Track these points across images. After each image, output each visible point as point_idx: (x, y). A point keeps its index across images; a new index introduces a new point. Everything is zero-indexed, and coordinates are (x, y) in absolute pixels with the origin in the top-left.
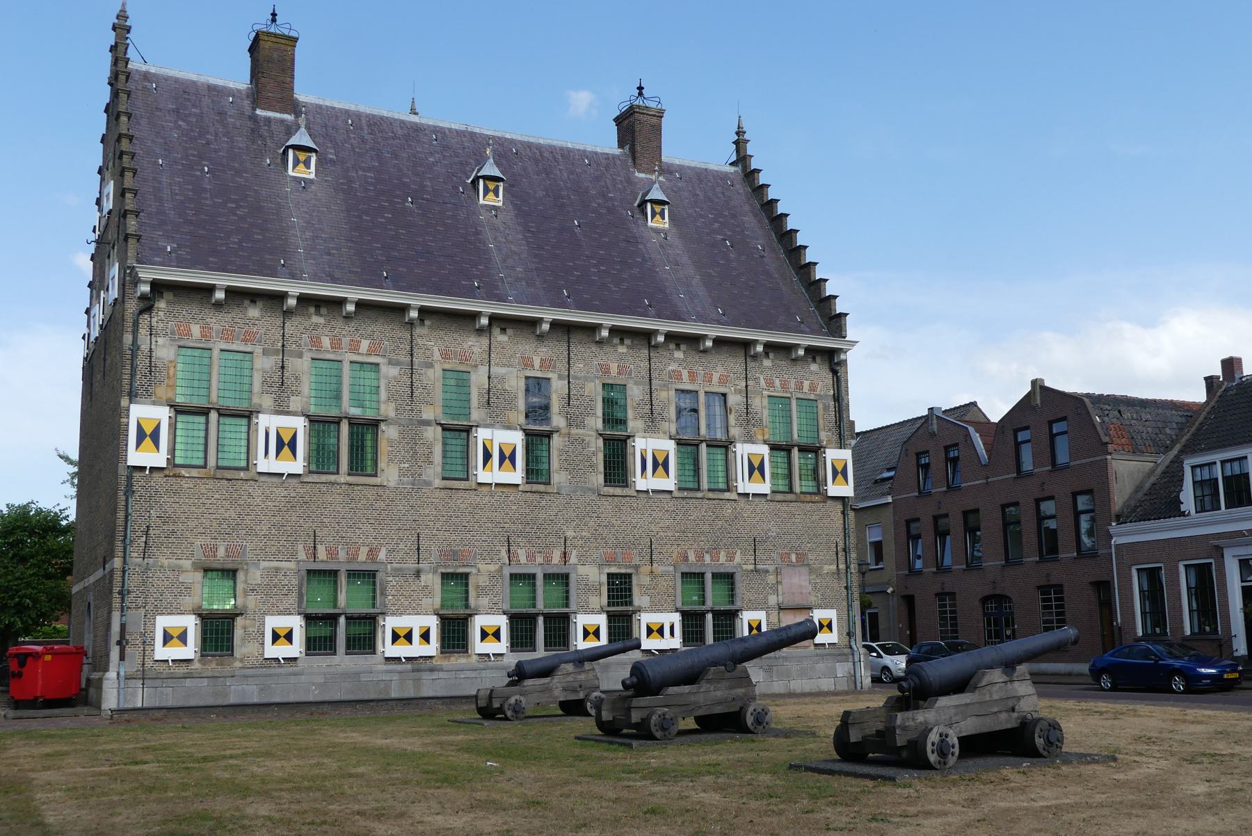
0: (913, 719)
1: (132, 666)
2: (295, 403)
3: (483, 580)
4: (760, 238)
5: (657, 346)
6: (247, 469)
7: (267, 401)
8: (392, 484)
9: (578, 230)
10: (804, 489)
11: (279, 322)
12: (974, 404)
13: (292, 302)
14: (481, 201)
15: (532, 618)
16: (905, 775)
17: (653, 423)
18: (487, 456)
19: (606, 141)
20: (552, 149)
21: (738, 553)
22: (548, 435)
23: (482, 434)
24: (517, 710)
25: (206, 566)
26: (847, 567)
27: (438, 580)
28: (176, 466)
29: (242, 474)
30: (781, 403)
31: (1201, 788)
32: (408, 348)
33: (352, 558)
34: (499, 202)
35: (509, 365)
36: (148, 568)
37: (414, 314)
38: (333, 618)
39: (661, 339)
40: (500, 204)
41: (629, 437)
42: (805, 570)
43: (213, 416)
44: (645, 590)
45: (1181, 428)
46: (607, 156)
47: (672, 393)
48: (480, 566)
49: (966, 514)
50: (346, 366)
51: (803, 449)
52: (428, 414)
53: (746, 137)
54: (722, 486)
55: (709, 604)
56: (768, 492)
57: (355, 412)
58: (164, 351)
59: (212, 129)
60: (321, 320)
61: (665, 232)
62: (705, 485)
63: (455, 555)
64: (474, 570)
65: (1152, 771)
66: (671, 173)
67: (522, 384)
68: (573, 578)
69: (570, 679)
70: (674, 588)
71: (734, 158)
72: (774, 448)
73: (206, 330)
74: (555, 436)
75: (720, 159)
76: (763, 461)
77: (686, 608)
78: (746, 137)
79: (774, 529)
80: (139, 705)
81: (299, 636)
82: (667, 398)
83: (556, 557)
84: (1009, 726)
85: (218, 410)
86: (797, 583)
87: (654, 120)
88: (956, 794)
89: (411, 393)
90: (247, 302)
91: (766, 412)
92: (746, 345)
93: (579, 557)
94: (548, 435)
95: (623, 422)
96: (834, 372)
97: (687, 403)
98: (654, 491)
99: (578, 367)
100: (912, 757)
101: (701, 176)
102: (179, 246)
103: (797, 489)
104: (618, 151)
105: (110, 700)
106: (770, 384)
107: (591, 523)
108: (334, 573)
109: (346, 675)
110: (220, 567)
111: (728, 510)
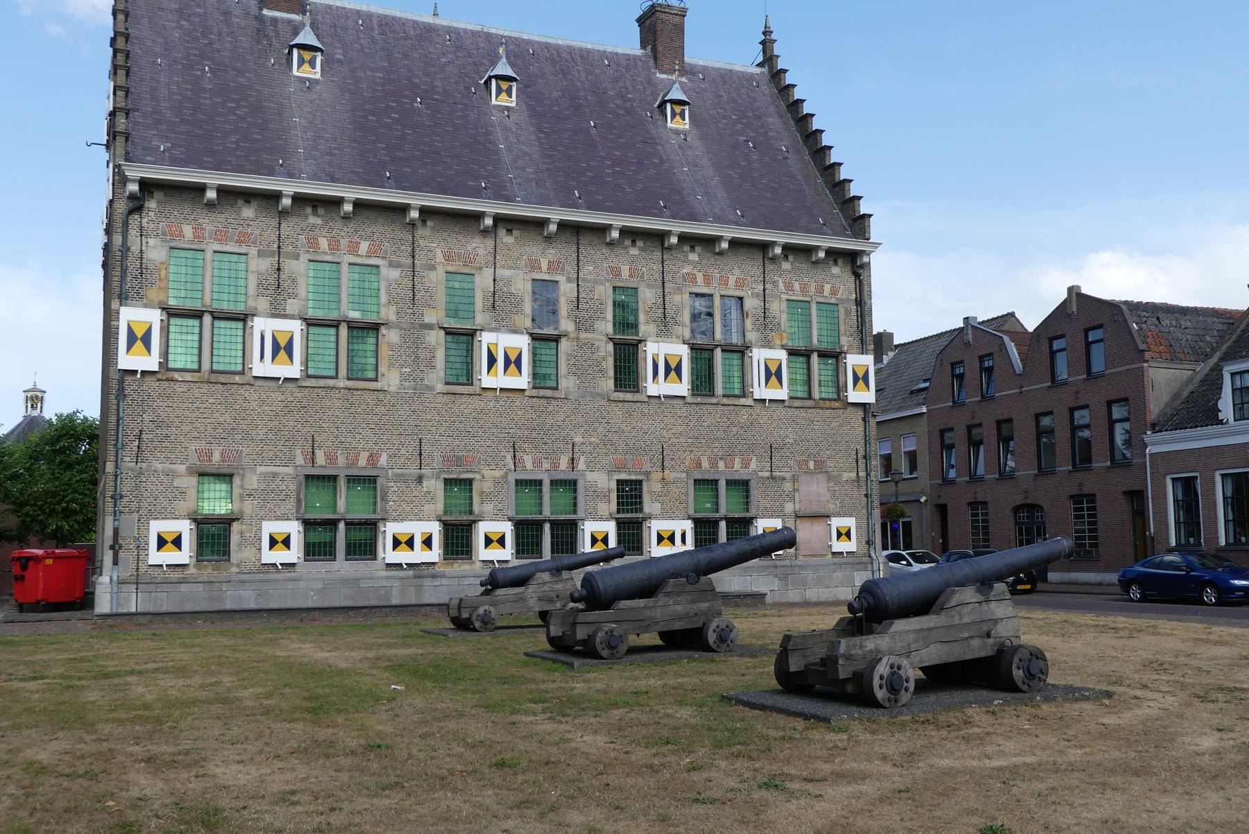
0: (861, 647)
1: (126, 570)
2: (292, 306)
3: (487, 486)
4: (785, 140)
5: (670, 248)
6: (242, 373)
7: (263, 304)
8: (393, 389)
9: (593, 131)
10: (824, 396)
11: (274, 223)
12: (1012, 315)
13: (287, 202)
14: (494, 102)
15: (539, 525)
16: (841, 714)
17: (665, 327)
18: (492, 360)
19: (628, 42)
20: (571, 50)
21: (754, 459)
22: (556, 339)
23: (486, 338)
24: (486, 621)
25: (201, 470)
26: (868, 475)
27: (441, 485)
28: (168, 370)
29: (237, 379)
30: (799, 307)
31: (1208, 742)
32: (410, 249)
33: (352, 464)
34: (512, 102)
35: (517, 268)
36: (141, 473)
37: (414, 214)
38: (333, 524)
39: (674, 240)
40: (514, 105)
41: (640, 341)
42: (823, 478)
43: (207, 319)
44: (656, 497)
45: (1222, 336)
46: (628, 57)
47: (686, 296)
48: (485, 472)
49: (999, 423)
50: (345, 268)
51: (823, 355)
52: (430, 317)
53: (773, 36)
54: (737, 392)
55: (723, 511)
56: (786, 398)
57: (355, 315)
58: (155, 252)
59: (215, 29)
60: (319, 221)
61: (685, 133)
62: (719, 390)
63: (458, 461)
64: (478, 477)
65: (1153, 712)
66: (694, 74)
67: (529, 286)
68: (580, 485)
69: (546, 588)
70: (687, 495)
71: (760, 59)
72: (792, 353)
73: (198, 230)
74: (563, 341)
75: (746, 60)
76: (780, 366)
77: (698, 515)
78: (773, 36)
80: (133, 610)
81: (297, 542)
82: (682, 304)
83: (564, 463)
84: (983, 654)
85: (211, 313)
86: (815, 491)
87: (677, 19)
88: (893, 744)
89: (413, 296)
90: (241, 202)
91: (784, 317)
92: (764, 247)
93: (588, 463)
94: (556, 339)
95: (634, 326)
96: (857, 276)
97: (700, 305)
98: (665, 397)
99: (588, 270)
100: (855, 693)
101: (726, 77)
102: (174, 146)
103: (816, 395)
104: (639, 52)
105: (103, 604)
106: (789, 287)
107: (601, 429)
108: (333, 479)
109: (345, 581)
110: (215, 471)
111: (744, 416)
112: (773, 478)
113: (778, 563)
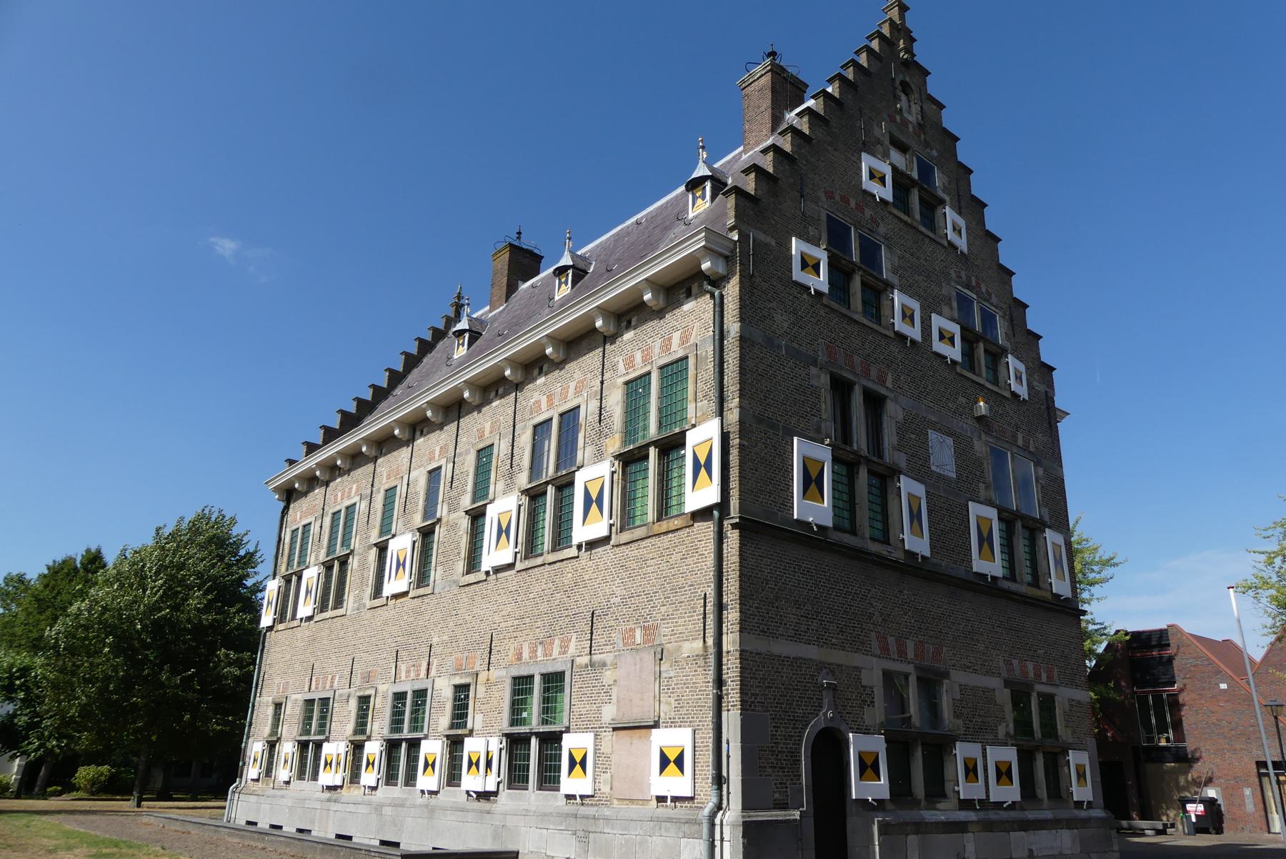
106: (630, 364)
112: (592, 664)
113: (583, 810)
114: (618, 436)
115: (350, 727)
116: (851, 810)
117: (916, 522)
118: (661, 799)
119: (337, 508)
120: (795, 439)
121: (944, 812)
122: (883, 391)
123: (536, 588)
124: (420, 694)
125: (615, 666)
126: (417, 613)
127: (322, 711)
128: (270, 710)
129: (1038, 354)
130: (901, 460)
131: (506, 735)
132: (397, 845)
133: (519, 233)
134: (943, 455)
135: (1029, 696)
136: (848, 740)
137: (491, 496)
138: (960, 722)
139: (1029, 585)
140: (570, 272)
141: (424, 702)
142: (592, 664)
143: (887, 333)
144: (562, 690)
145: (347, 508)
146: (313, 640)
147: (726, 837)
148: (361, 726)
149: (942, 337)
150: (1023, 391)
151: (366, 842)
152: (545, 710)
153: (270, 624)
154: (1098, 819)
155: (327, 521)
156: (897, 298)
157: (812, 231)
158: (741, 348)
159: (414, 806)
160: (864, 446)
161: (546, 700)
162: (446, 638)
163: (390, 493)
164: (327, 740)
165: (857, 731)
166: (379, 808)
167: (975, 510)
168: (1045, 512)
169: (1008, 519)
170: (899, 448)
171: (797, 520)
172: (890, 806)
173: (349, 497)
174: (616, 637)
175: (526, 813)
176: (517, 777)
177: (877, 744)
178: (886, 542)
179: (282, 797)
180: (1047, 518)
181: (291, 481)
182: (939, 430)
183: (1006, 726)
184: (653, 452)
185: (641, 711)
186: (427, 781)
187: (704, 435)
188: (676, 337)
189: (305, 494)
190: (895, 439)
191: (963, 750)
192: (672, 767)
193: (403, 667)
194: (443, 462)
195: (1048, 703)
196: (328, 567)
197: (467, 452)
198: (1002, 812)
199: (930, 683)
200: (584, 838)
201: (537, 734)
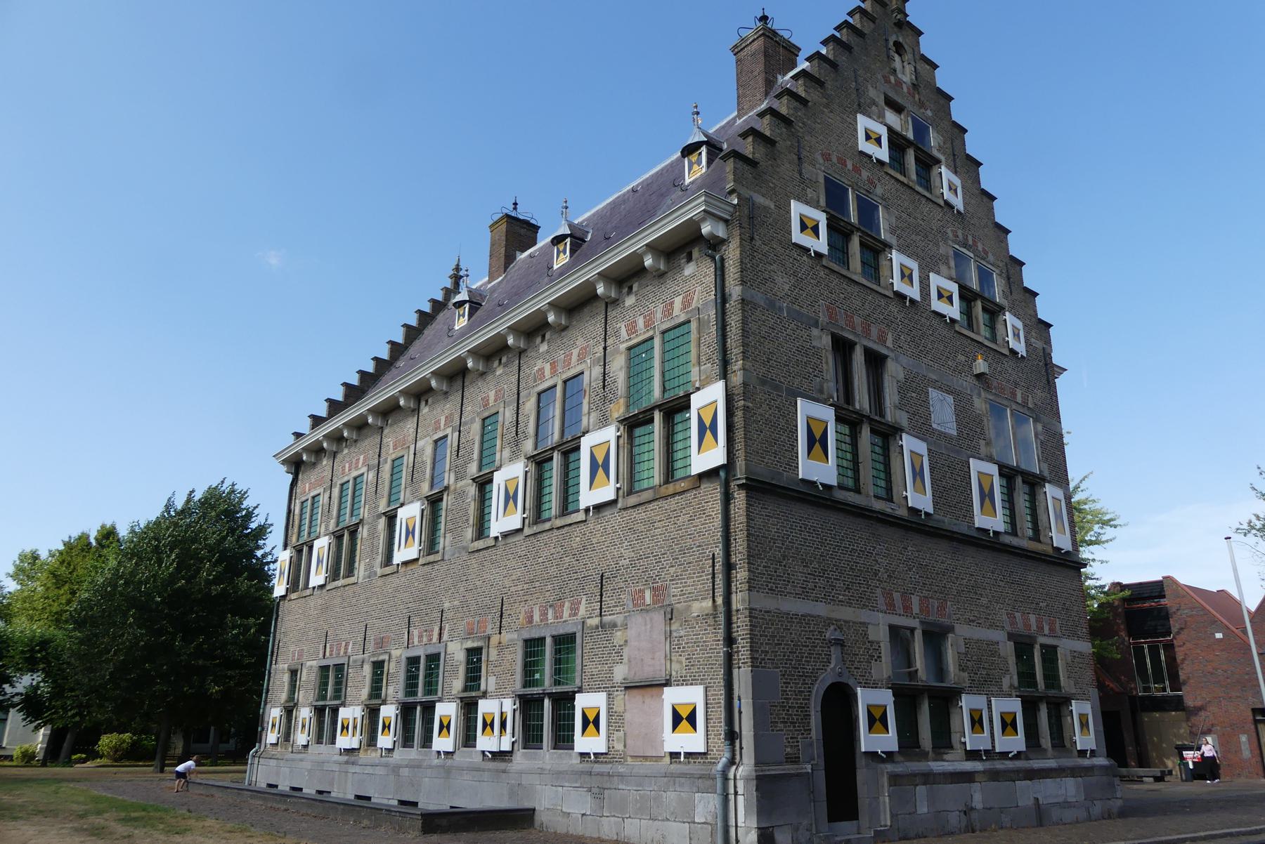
79: (627, 554)
106: (632, 329)
112: (602, 625)
113: (598, 768)
114: (622, 401)
115: (365, 692)
116: (861, 762)
117: (918, 478)
118: (674, 755)
119: (346, 479)
120: (799, 401)
121: (953, 763)
122: (884, 351)
123: (545, 553)
124: (433, 659)
125: (625, 627)
126: (428, 579)
127: (337, 677)
128: (286, 678)
129: (1035, 311)
130: (903, 419)
131: (520, 697)
132: (415, 804)
133: (515, 204)
134: (943, 413)
135: (1031, 646)
136: (856, 694)
137: (497, 463)
138: (966, 674)
139: (1030, 539)
140: (568, 240)
141: (438, 666)
142: (602, 625)
143: (887, 293)
144: (573, 650)
145: (355, 479)
146: (325, 608)
147: (740, 791)
148: (376, 691)
149: (940, 296)
150: (1021, 348)
151: (385, 802)
152: (557, 672)
153: (283, 593)
154: (1102, 767)
155: (336, 491)
156: (897, 258)
157: (810, 193)
158: (743, 310)
159: (430, 767)
160: (866, 406)
161: (557, 661)
162: (456, 603)
163: (396, 463)
164: (343, 705)
165: (866, 685)
166: (396, 769)
167: (976, 466)
168: (1045, 467)
169: (1008, 474)
170: (899, 407)
171: (802, 480)
172: (898, 758)
173: (357, 468)
174: (625, 597)
175: (541, 772)
176: (531, 737)
177: (885, 698)
178: (890, 500)
179: (301, 760)
180: (1046, 474)
181: (298, 454)
182: (940, 388)
183: (1010, 679)
184: (657, 416)
185: (654, 668)
186: (443, 743)
187: (709, 397)
188: (678, 301)
189: (314, 465)
190: (896, 398)
191: (967, 702)
192: (685, 723)
193: (415, 633)
194: (449, 431)
195: (1050, 654)
196: (338, 537)
197: (473, 421)
198: (1007, 762)
199: (935, 637)
200: (599, 794)
201: (550, 695)
